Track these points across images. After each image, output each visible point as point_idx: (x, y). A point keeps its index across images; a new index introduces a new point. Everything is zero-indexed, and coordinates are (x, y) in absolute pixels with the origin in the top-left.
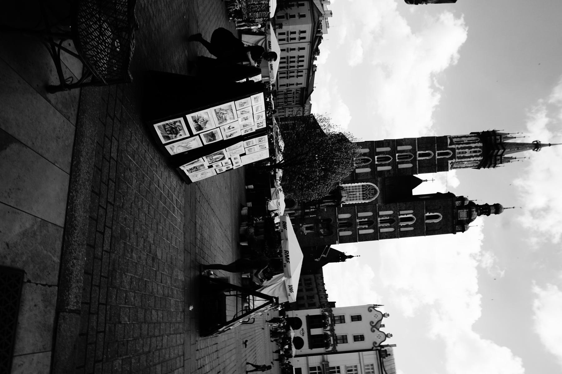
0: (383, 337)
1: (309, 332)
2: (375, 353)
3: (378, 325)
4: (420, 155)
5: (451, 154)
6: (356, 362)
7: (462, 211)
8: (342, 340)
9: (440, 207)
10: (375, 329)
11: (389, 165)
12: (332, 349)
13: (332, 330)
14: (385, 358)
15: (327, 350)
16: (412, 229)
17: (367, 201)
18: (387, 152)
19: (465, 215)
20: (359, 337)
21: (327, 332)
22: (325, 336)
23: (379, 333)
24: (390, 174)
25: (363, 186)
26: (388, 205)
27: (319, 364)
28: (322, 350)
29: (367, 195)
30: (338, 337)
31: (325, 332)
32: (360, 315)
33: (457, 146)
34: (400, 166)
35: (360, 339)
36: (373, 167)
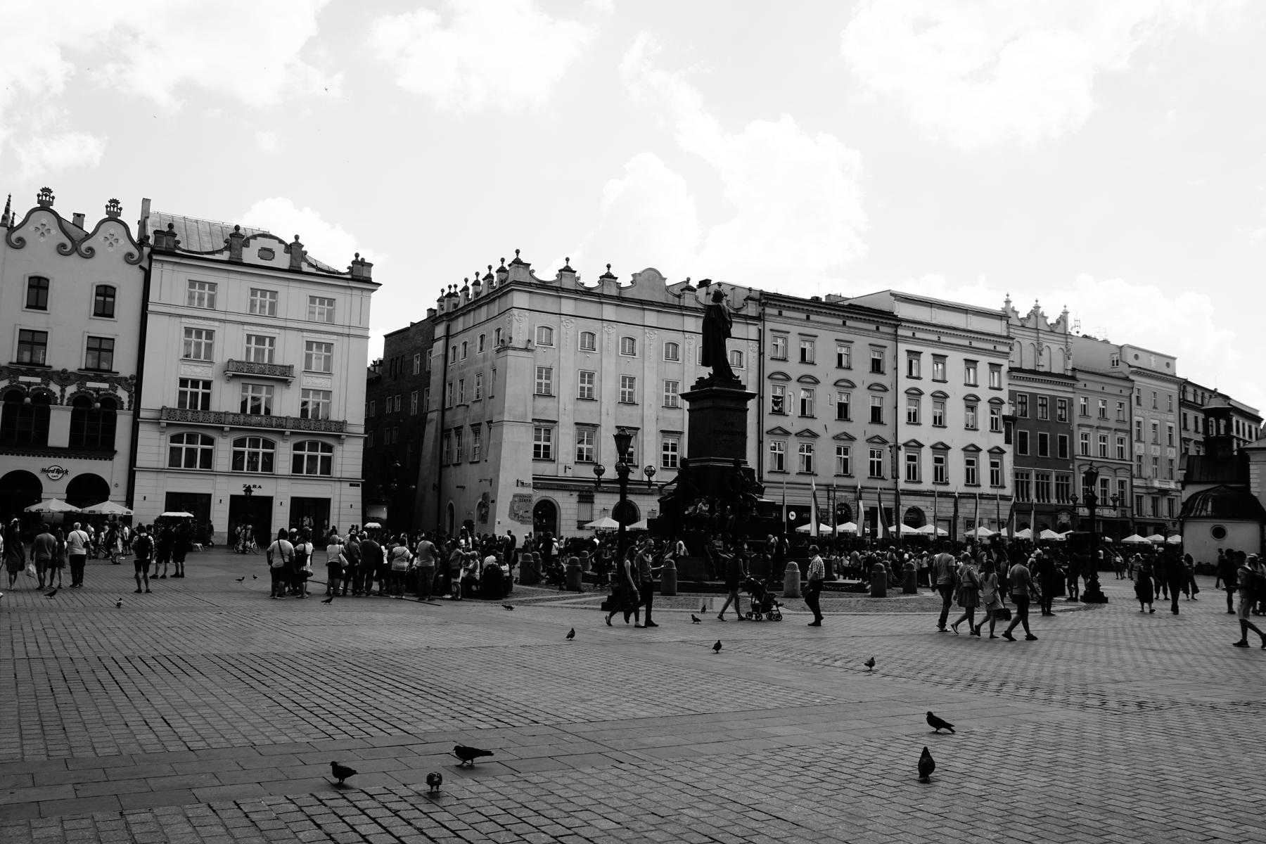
0: (112, 228)
1: (58, 452)
2: (159, 265)
3: (74, 231)
6: (178, 327)
8: (103, 354)
10: (84, 246)
12: (124, 389)
13: (64, 377)
14: (178, 242)
15: (126, 406)
20: (102, 298)
21: (67, 395)
22: (80, 403)
23: (100, 237)
27: (164, 437)
28: (123, 422)
30: (90, 366)
31: (65, 401)
32: (30, 278)
35: (108, 299)
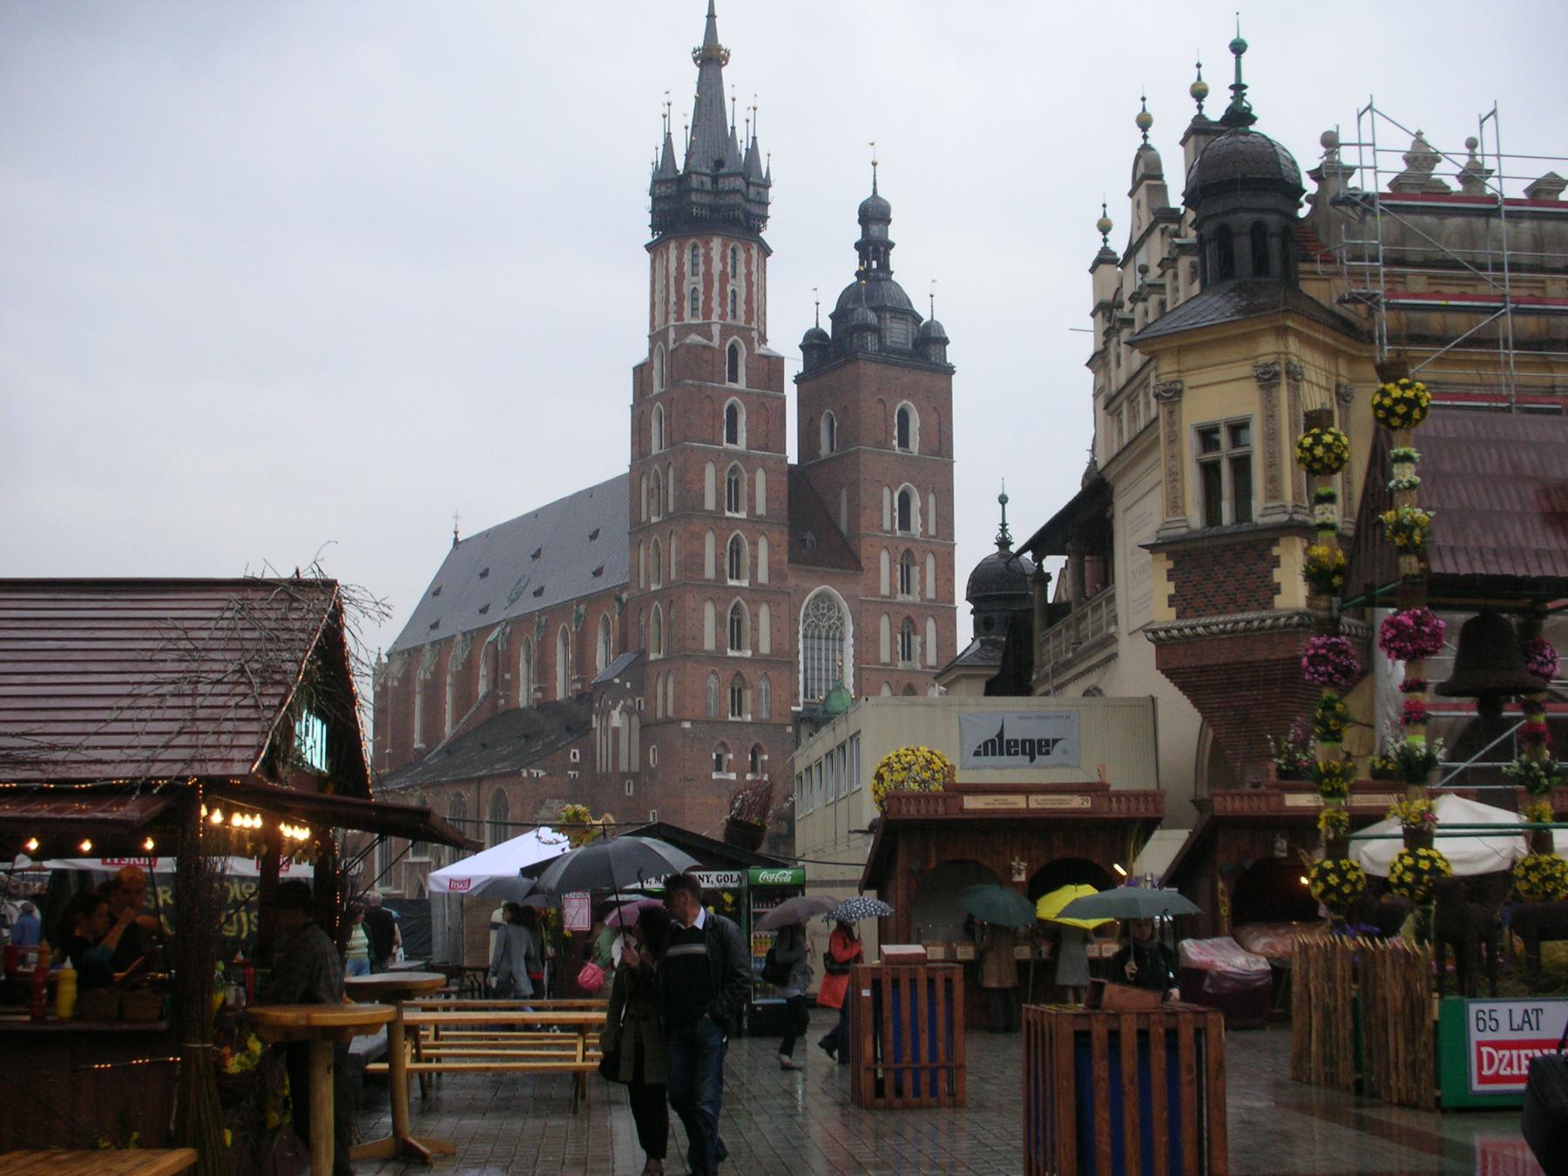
4: (732, 439)
5: (736, 341)
7: (888, 332)
9: (881, 401)
11: (754, 544)
16: (932, 499)
17: (850, 629)
18: (717, 546)
19: (900, 326)
24: (779, 546)
25: (805, 636)
26: (864, 564)
29: (830, 627)
33: (715, 318)
34: (761, 509)
36: (757, 593)
